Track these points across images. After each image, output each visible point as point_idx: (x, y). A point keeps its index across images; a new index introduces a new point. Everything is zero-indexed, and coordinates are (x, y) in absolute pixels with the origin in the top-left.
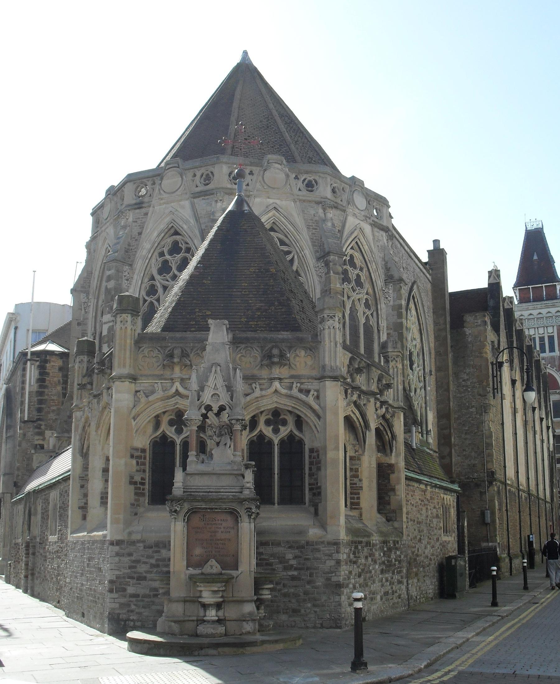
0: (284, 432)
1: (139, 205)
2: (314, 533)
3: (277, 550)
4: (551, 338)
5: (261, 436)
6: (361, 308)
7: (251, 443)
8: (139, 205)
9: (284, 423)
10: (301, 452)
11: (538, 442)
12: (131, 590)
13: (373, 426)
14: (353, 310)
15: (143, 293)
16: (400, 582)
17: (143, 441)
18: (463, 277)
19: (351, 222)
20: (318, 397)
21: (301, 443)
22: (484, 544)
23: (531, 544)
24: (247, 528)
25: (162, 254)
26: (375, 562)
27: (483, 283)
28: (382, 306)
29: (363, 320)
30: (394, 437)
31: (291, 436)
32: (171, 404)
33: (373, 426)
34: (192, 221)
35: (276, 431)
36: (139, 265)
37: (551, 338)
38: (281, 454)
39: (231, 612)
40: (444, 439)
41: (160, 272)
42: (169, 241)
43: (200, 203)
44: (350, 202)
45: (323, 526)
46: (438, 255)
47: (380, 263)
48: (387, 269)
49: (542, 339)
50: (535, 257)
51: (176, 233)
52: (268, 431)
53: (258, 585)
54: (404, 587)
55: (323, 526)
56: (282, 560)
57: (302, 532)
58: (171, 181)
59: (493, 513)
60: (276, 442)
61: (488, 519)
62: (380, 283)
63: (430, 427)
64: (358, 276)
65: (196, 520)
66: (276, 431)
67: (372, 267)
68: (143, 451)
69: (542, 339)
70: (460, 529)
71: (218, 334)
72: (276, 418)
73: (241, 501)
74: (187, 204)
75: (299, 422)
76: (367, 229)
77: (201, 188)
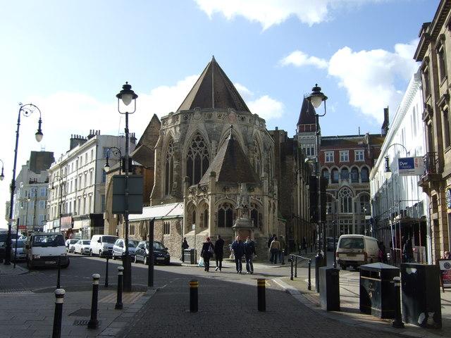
2: (261, 235)
4: (313, 149)
6: (256, 159)
17: (217, 211)
19: (255, 130)
23: (304, 240)
25: (193, 140)
28: (262, 158)
32: (224, 201)
34: (205, 131)
37: (313, 149)
41: (193, 146)
43: (208, 125)
44: (255, 124)
45: (263, 233)
48: (265, 146)
49: (308, 149)
50: (308, 111)
51: (198, 133)
55: (263, 233)
62: (262, 151)
67: (260, 145)
69: (308, 149)
74: (203, 124)
76: (259, 131)
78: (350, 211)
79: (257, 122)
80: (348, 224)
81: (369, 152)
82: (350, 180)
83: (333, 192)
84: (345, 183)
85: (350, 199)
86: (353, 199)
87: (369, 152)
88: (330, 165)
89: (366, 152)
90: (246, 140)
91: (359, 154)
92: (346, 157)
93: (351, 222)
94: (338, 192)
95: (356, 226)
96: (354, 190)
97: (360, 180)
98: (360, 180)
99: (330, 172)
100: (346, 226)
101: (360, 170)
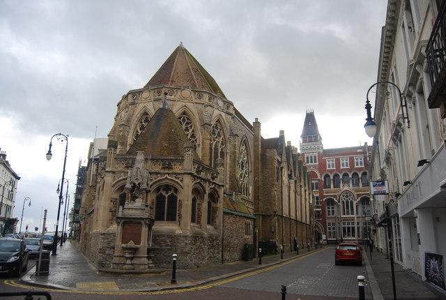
0: (170, 193)
1: (133, 104)
2: (179, 232)
3: (163, 238)
4: (315, 157)
5: (161, 194)
7: (157, 197)
8: (133, 104)
9: (170, 190)
10: (176, 200)
11: (303, 200)
12: (107, 252)
13: (207, 192)
14: (216, 146)
15: (134, 137)
16: (218, 253)
18: (268, 132)
20: (182, 181)
21: (176, 197)
22: (271, 240)
24: (145, 230)
26: (205, 244)
27: (277, 136)
29: (220, 150)
30: (219, 197)
31: (172, 195)
33: (207, 192)
35: (167, 193)
36: (132, 127)
37: (315, 157)
38: (169, 201)
39: (136, 261)
40: (256, 197)
42: (144, 117)
43: (156, 103)
46: (257, 124)
47: (228, 128)
49: (311, 157)
52: (164, 193)
53: (149, 251)
54: (220, 256)
56: (165, 242)
57: (173, 232)
58: (145, 95)
59: (275, 228)
60: (167, 196)
61: (273, 230)
62: (227, 136)
63: (250, 192)
64: (219, 132)
65: (126, 226)
66: (167, 193)
67: (225, 129)
68: (116, 199)
69: (311, 157)
70: (255, 233)
71: (140, 157)
72: (167, 188)
73: (141, 219)
75: (176, 190)
76: (223, 114)
77: (157, 97)
78: (352, 214)
79: (221, 103)
80: (351, 226)
81: (368, 158)
82: (351, 185)
83: (335, 196)
84: (346, 188)
85: (352, 203)
86: (355, 203)
87: (368, 158)
88: (331, 171)
89: (365, 159)
90: (201, 120)
91: (359, 160)
92: (347, 163)
93: (353, 224)
94: (339, 196)
95: (358, 228)
96: (355, 194)
97: (361, 185)
98: (361, 185)
99: (332, 178)
100: (349, 228)
101: (360, 176)
